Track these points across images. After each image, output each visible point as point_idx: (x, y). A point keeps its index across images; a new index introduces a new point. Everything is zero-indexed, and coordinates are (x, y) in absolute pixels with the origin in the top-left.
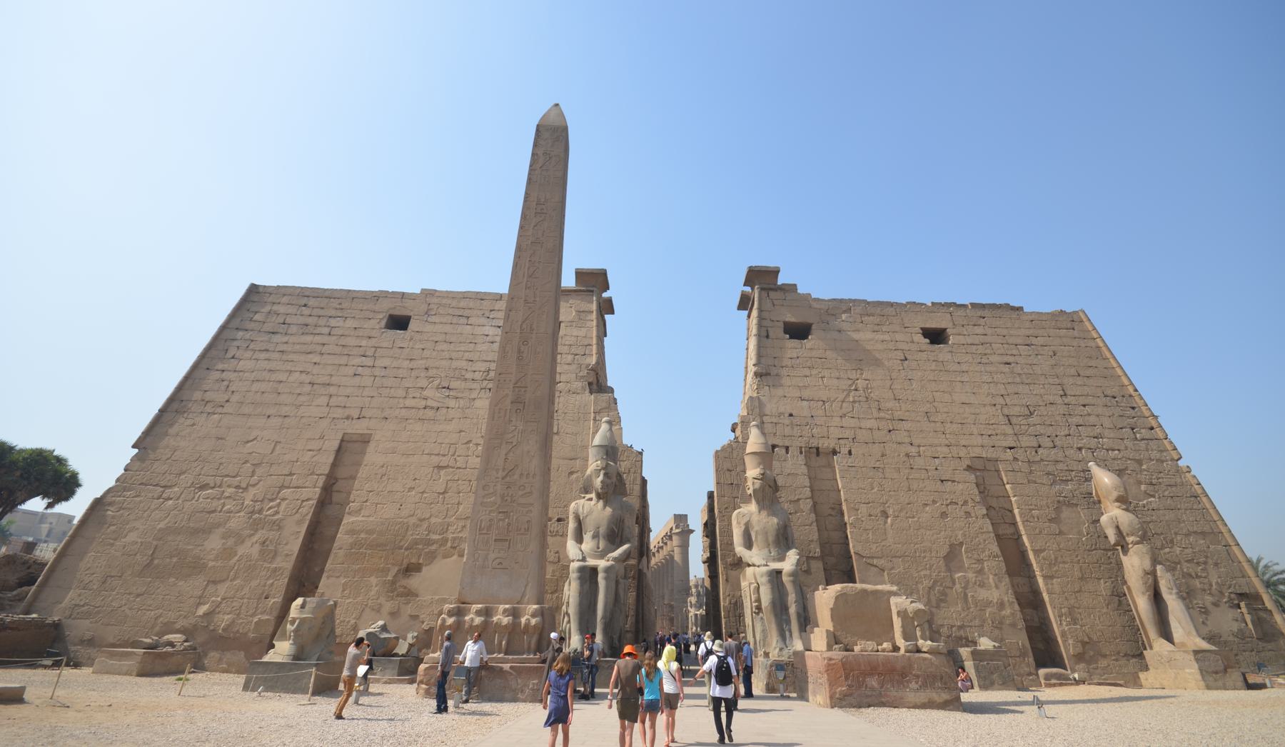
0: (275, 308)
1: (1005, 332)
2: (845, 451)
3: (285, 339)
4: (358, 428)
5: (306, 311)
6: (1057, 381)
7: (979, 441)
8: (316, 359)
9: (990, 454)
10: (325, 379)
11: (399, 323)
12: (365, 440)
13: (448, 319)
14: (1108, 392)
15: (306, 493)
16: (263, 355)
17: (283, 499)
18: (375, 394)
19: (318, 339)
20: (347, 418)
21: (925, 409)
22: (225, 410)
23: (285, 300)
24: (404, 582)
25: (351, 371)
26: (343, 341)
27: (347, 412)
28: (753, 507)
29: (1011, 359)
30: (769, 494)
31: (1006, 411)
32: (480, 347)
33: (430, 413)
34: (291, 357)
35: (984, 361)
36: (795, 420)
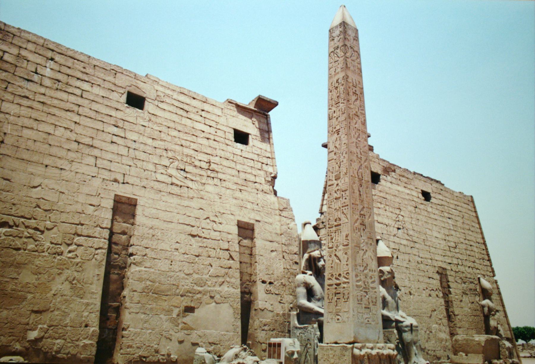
3: (43, 90)
4: (125, 191)
6: (463, 231)
7: (441, 258)
8: (76, 118)
10: (88, 141)
11: (136, 101)
12: (132, 204)
13: (172, 109)
15: (97, 243)
16: (25, 102)
17: (79, 245)
18: (132, 164)
19: (72, 98)
20: (116, 181)
21: (423, 238)
24: (185, 320)
25: (109, 138)
26: (95, 106)
27: (113, 176)
32: (200, 141)
33: (175, 190)
35: (442, 215)
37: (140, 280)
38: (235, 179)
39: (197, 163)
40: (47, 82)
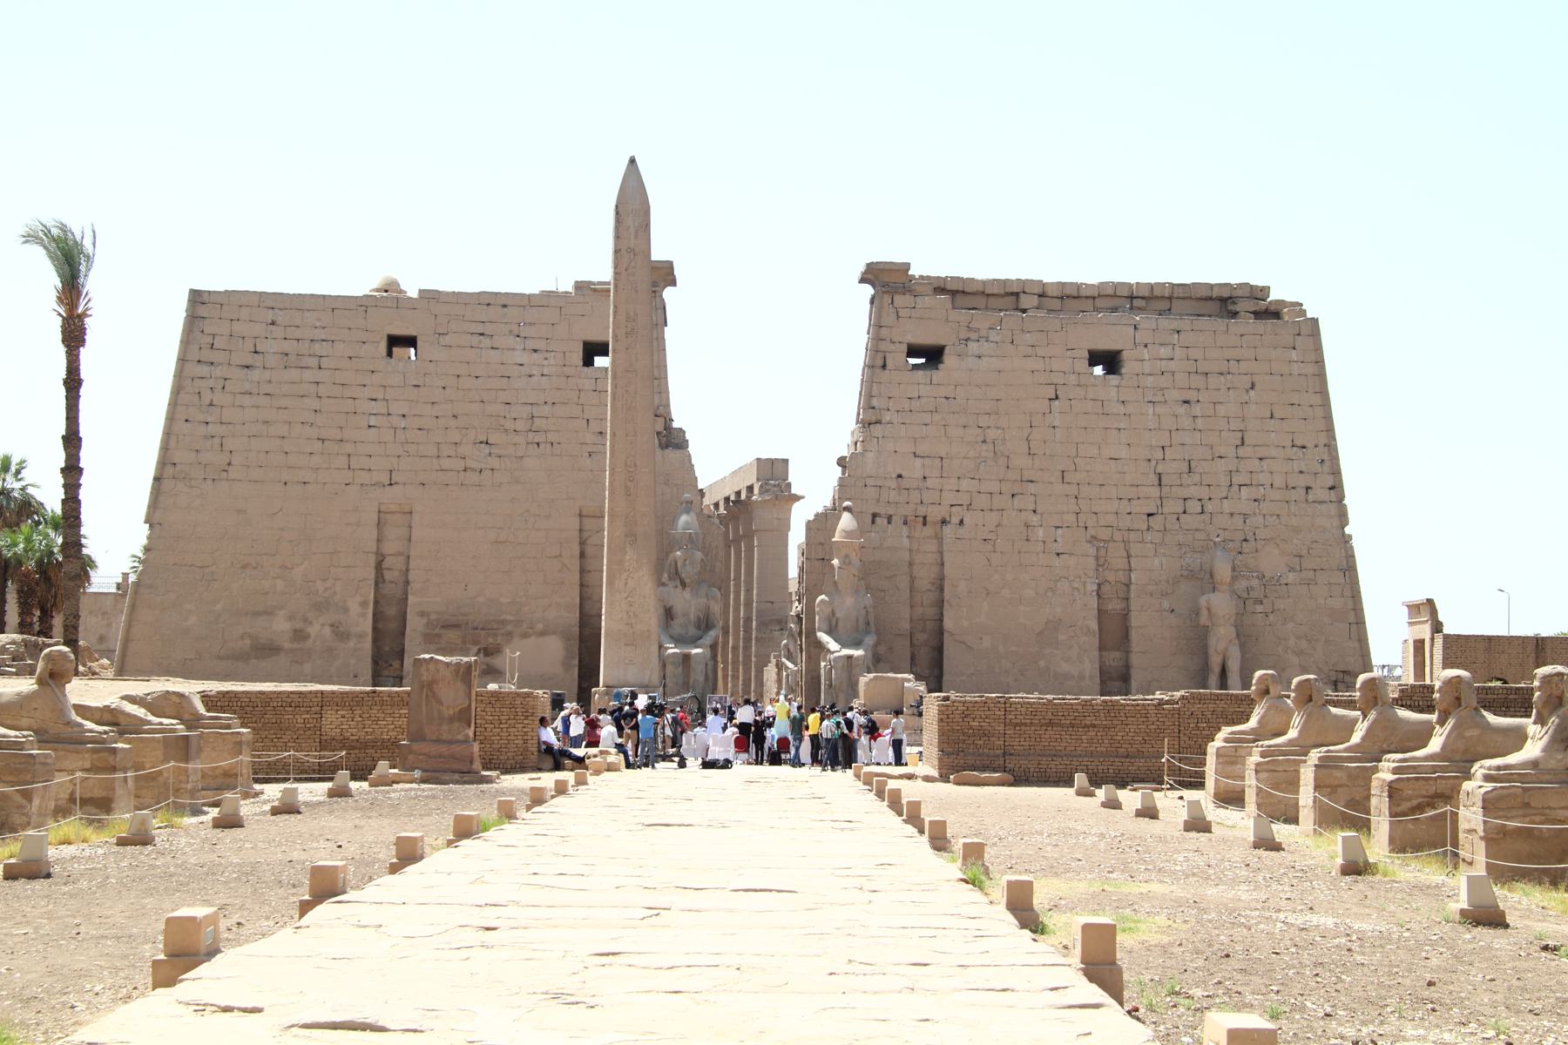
0: (237, 327)
1: (1194, 354)
2: (955, 520)
3: (267, 375)
5: (278, 332)
8: (316, 404)
9: (1126, 522)
14: (1298, 442)
16: (247, 401)
18: (401, 452)
19: (309, 375)
22: (232, 475)
23: (244, 314)
29: (1192, 395)
31: (1160, 470)
33: (472, 477)
36: (904, 483)
37: (422, 614)
39: (509, 425)
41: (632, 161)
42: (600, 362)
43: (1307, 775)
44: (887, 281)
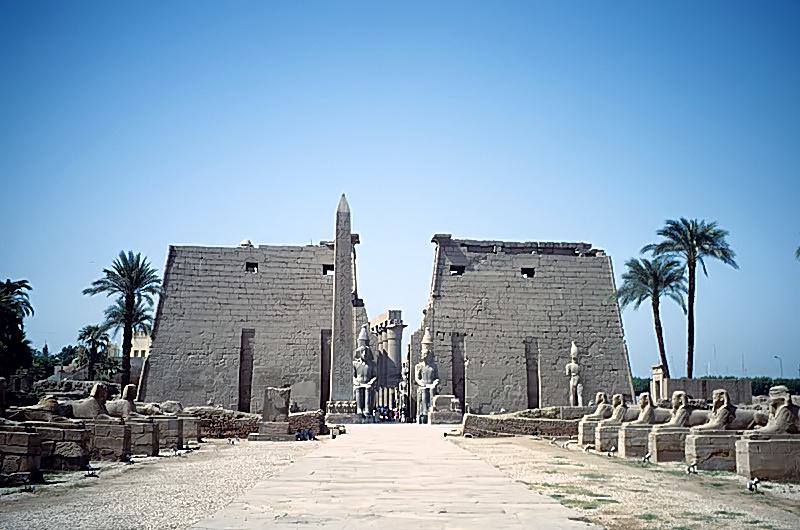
0: (187, 260)
3: (199, 279)
4: (248, 326)
8: (218, 290)
11: (251, 266)
12: (253, 332)
13: (277, 265)
16: (191, 289)
19: (214, 278)
20: (242, 320)
23: (190, 255)
28: (423, 363)
30: (429, 360)
32: (296, 281)
33: (279, 318)
34: (205, 289)
38: (322, 302)
39: (294, 298)
40: (201, 273)
41: (344, 195)
42: (329, 272)
43: (622, 434)
44: (442, 241)
